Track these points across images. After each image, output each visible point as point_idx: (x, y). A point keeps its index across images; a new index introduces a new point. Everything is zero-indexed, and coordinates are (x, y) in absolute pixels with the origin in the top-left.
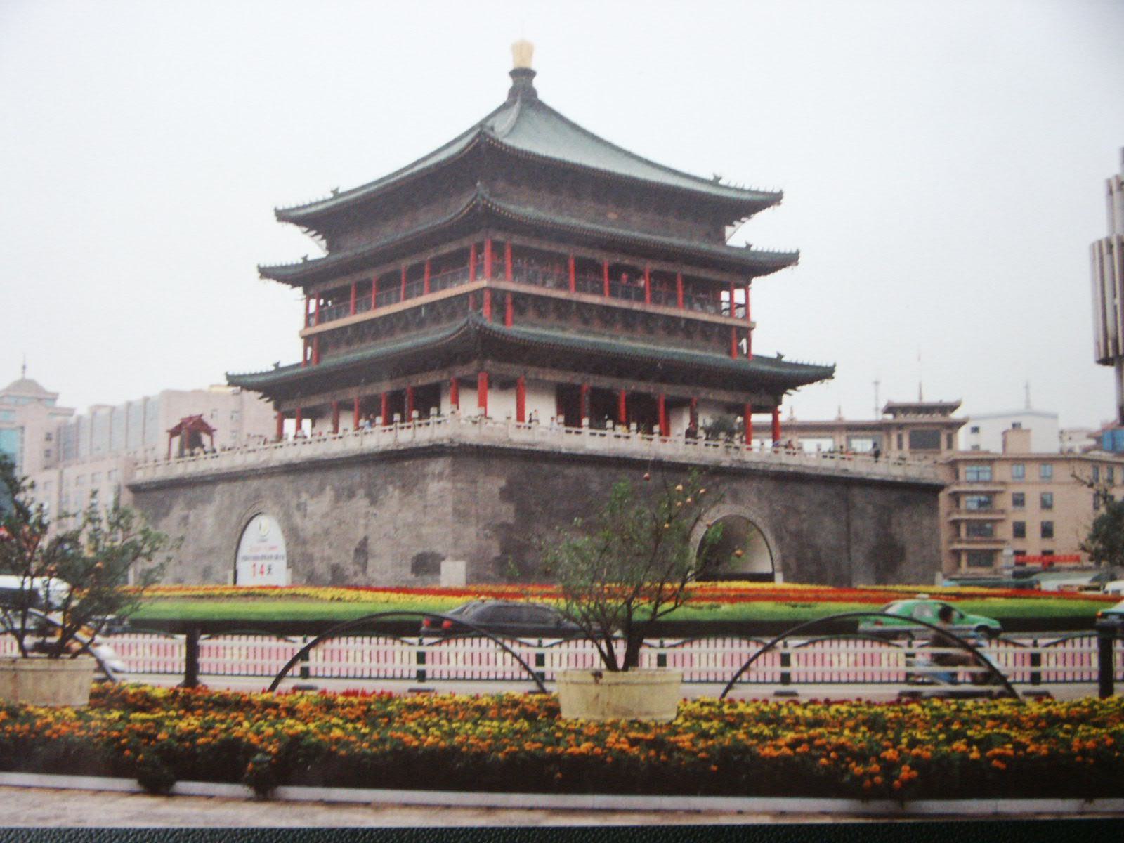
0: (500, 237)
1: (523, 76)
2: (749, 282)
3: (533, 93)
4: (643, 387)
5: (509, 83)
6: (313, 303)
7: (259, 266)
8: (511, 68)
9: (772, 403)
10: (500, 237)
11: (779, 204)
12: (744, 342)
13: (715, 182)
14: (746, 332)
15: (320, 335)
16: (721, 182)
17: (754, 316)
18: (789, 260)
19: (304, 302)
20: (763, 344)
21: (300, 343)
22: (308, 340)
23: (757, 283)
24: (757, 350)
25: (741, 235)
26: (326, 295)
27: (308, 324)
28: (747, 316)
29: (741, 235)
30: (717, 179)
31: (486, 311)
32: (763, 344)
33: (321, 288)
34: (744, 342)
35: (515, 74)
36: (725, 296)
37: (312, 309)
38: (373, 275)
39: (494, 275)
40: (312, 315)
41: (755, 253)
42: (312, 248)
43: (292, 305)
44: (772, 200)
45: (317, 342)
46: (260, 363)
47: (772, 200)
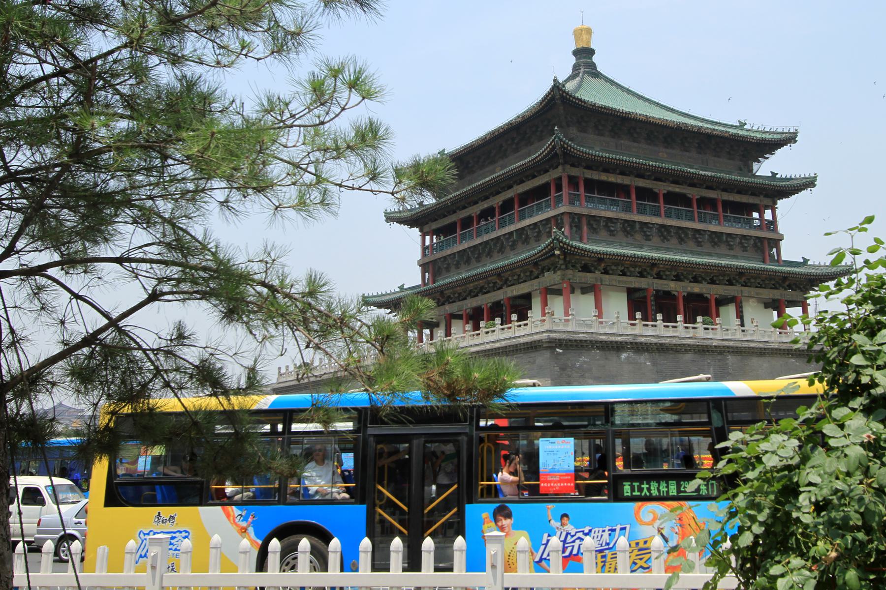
0: (575, 172)
1: (584, 55)
3: (593, 66)
4: (696, 288)
5: (573, 60)
6: (428, 238)
7: (386, 212)
8: (574, 48)
10: (575, 172)
11: (795, 142)
12: (774, 250)
13: (742, 125)
14: (776, 243)
15: (434, 262)
16: (745, 127)
17: (781, 230)
18: (809, 183)
19: (419, 239)
20: (789, 251)
21: (419, 270)
23: (781, 204)
24: (784, 257)
25: (764, 168)
26: (437, 232)
27: (424, 254)
28: (775, 230)
29: (764, 168)
31: (566, 230)
32: (789, 251)
33: (435, 226)
34: (774, 250)
35: (576, 53)
36: (756, 215)
37: (428, 243)
38: (474, 210)
39: (572, 203)
40: (427, 247)
41: (781, 179)
43: (410, 242)
44: (790, 139)
47: (790, 139)
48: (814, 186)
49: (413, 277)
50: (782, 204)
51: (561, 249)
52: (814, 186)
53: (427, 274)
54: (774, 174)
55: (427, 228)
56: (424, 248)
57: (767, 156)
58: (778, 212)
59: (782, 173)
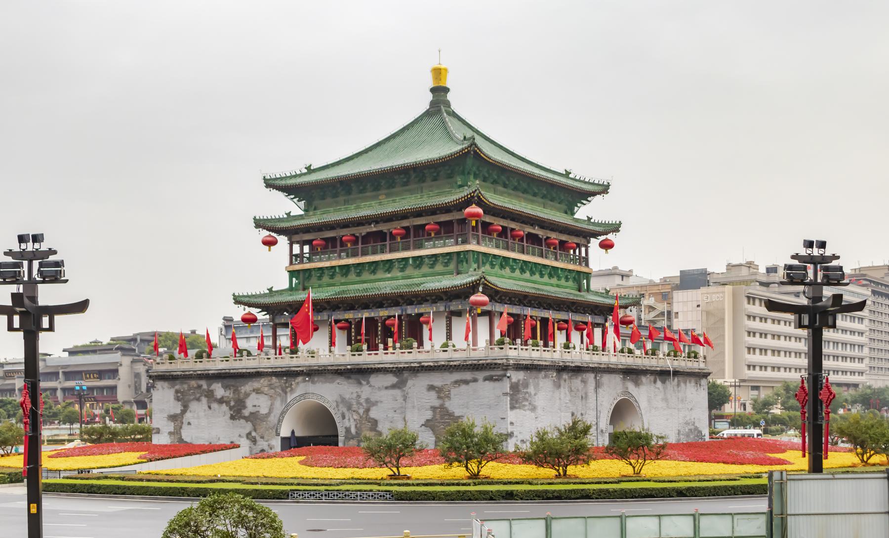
2: (589, 242)
7: (255, 218)
9: (603, 322)
13: (567, 174)
16: (571, 176)
21: (287, 275)
22: (292, 274)
25: (582, 212)
27: (291, 263)
28: (587, 265)
30: (567, 174)
40: (296, 256)
42: (287, 207)
44: (604, 189)
45: (301, 277)
46: (257, 287)
47: (604, 189)
48: (618, 231)
49: (282, 282)
50: (594, 243)
51: (485, 286)
52: (618, 231)
53: (294, 279)
54: (589, 219)
55: (296, 238)
56: (291, 255)
57: (584, 202)
58: (590, 250)
59: (596, 218)
